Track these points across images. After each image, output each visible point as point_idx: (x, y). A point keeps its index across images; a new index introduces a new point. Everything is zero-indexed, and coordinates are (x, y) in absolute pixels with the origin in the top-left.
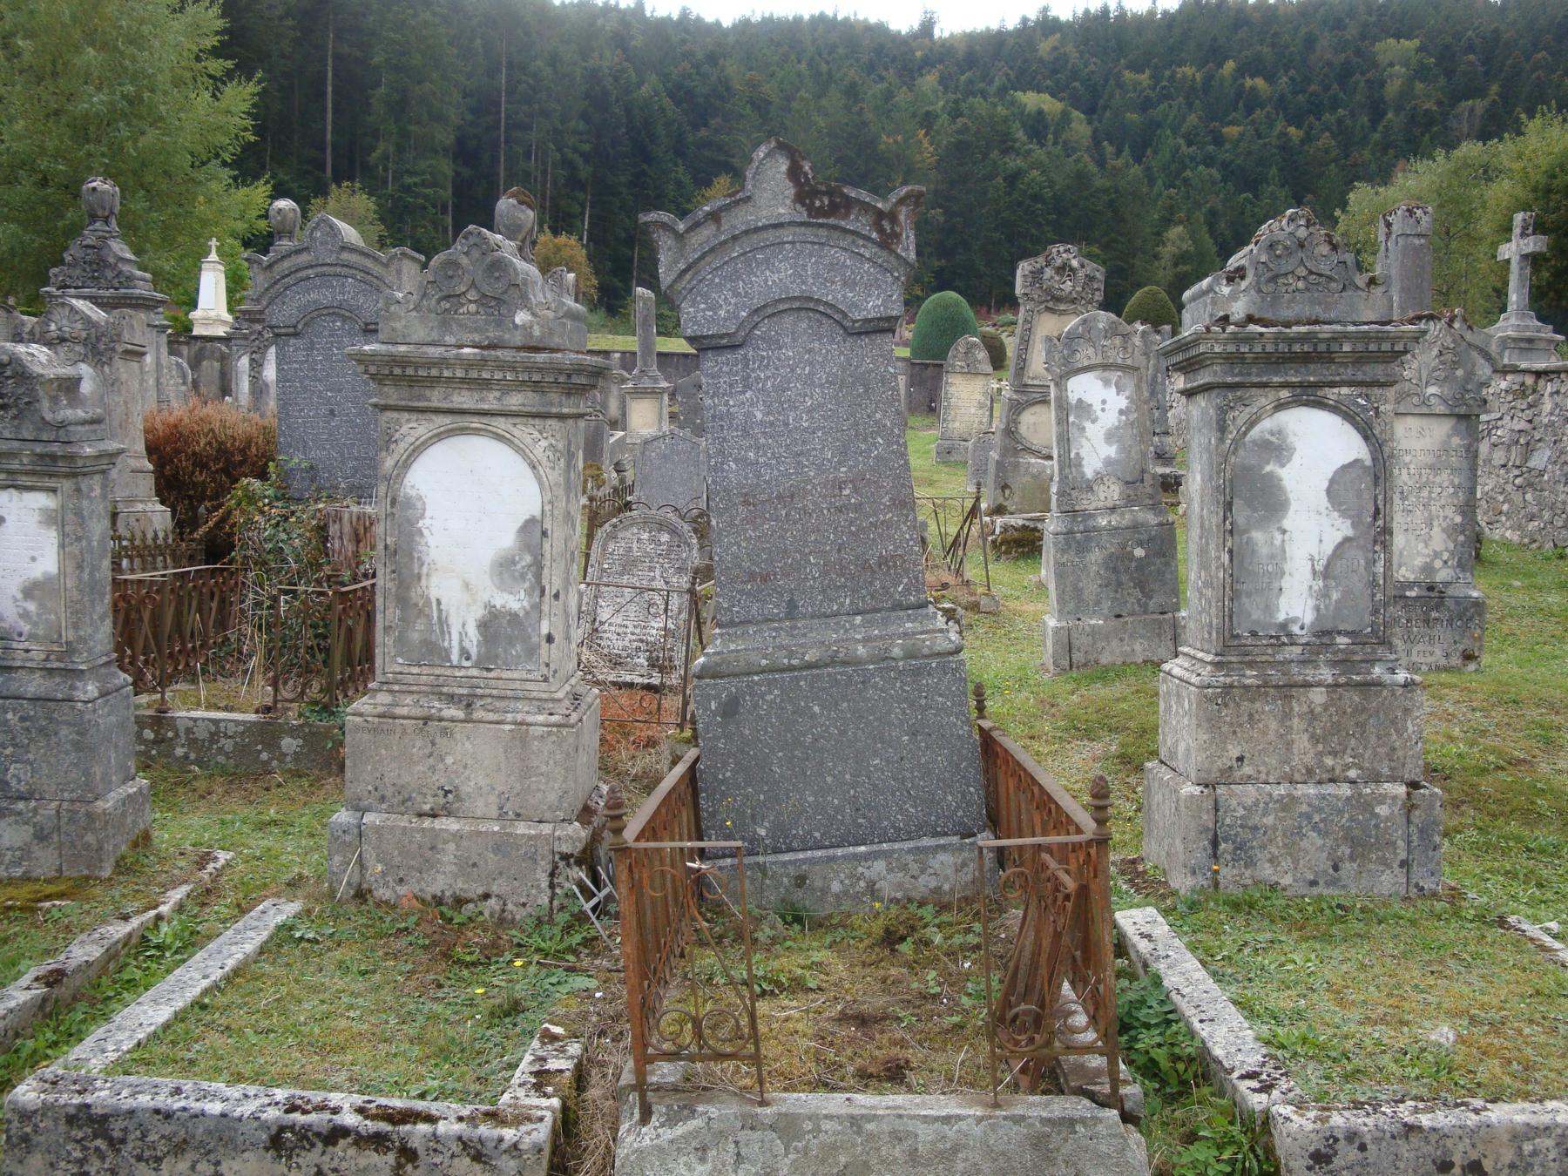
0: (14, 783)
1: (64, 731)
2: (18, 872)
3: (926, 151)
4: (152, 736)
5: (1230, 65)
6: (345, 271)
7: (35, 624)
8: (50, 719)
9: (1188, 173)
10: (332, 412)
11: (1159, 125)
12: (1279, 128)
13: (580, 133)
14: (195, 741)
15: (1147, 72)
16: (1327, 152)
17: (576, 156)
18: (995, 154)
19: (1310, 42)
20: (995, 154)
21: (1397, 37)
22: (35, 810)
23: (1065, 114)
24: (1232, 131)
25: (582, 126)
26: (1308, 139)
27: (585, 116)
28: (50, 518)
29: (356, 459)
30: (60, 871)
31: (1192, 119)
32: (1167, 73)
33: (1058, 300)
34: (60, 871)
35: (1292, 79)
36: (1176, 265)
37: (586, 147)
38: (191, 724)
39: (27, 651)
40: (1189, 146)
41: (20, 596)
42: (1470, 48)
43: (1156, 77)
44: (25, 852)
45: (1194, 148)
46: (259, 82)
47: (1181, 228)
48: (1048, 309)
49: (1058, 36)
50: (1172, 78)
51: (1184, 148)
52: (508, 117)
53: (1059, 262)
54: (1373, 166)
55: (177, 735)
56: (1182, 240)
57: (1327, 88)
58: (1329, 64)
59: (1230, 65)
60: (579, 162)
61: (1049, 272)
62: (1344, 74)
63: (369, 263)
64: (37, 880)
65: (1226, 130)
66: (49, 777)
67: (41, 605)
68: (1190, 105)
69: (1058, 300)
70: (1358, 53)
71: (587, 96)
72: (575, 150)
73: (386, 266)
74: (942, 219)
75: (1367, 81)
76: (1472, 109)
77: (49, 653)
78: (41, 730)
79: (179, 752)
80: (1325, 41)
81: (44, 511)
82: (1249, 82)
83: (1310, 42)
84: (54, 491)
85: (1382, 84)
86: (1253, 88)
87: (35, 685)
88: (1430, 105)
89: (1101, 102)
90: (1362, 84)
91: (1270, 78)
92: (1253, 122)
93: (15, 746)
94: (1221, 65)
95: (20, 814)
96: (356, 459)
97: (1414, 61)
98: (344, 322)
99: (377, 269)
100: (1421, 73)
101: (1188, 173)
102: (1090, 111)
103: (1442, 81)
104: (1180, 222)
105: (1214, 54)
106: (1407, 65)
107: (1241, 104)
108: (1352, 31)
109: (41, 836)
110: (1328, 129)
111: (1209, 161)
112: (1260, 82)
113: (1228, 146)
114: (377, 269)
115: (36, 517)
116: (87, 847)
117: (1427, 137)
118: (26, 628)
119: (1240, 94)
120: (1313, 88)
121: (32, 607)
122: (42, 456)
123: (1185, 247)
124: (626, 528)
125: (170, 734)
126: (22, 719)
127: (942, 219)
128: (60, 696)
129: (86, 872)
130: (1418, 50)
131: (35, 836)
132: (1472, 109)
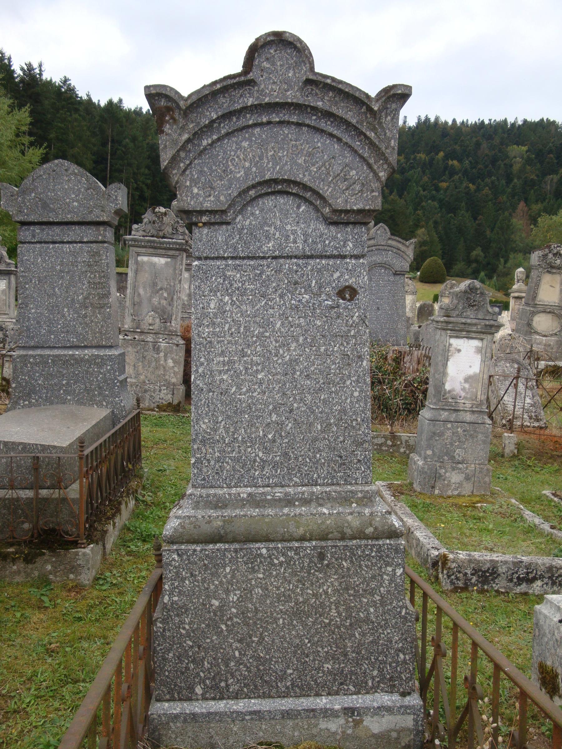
0: (457, 457)
1: (480, 436)
2: (456, 493)
4: (391, 443)
5: (441, 154)
6: (389, 248)
7: (467, 393)
8: (475, 431)
9: (424, 204)
10: (378, 308)
11: (409, 180)
12: (464, 185)
13: (146, 175)
14: (409, 446)
15: (403, 155)
16: (487, 196)
17: (144, 186)
21: (518, 145)
22: (467, 468)
24: (444, 185)
25: (147, 171)
26: (478, 190)
27: (148, 167)
28: (479, 350)
29: (388, 329)
30: (472, 492)
31: (425, 179)
32: (412, 157)
33: (552, 267)
34: (472, 492)
35: (470, 162)
36: (421, 246)
37: (149, 182)
38: (408, 438)
39: (464, 404)
40: (424, 191)
41: (463, 381)
42: (550, 152)
44: (460, 484)
45: (426, 192)
46: (45, 148)
47: (423, 229)
48: (548, 272)
50: (415, 159)
51: (422, 192)
52: (111, 166)
53: (555, 251)
54: (508, 204)
55: (401, 443)
56: (424, 235)
57: (486, 167)
58: (487, 155)
59: (441, 154)
60: (145, 188)
61: (550, 256)
62: (494, 161)
63: (400, 246)
64: (464, 496)
65: (440, 184)
66: (471, 454)
67: (471, 385)
68: (424, 172)
69: (552, 267)
70: (500, 151)
71: (149, 157)
72: (143, 183)
73: (408, 247)
75: (505, 164)
76: (552, 179)
77: (473, 404)
78: (471, 435)
79: (402, 450)
80: (485, 145)
81: (477, 347)
82: (450, 162)
83: (478, 145)
84: (482, 339)
85: (511, 166)
86: (452, 165)
87: (468, 417)
88: (532, 177)
90: (502, 166)
91: (460, 161)
92: (453, 181)
93: (459, 442)
94: (437, 154)
95: (460, 469)
96: (388, 329)
97: (525, 156)
98: (385, 270)
99: (403, 248)
100: (529, 161)
101: (424, 204)
103: (538, 165)
104: (422, 227)
105: (434, 149)
106: (522, 158)
107: (447, 172)
108: (497, 140)
109: (467, 478)
110: (487, 186)
111: (433, 198)
112: (455, 162)
113: (442, 192)
114: (403, 248)
115: (474, 350)
116: (485, 483)
117: (532, 191)
118: (463, 394)
119: (446, 168)
120: (480, 166)
121: (467, 386)
122: (486, 325)
123: (425, 238)
124: (499, 362)
125: (399, 443)
126: (464, 431)
128: (480, 422)
129: (483, 493)
130: (527, 152)
131: (465, 478)
132: (552, 179)
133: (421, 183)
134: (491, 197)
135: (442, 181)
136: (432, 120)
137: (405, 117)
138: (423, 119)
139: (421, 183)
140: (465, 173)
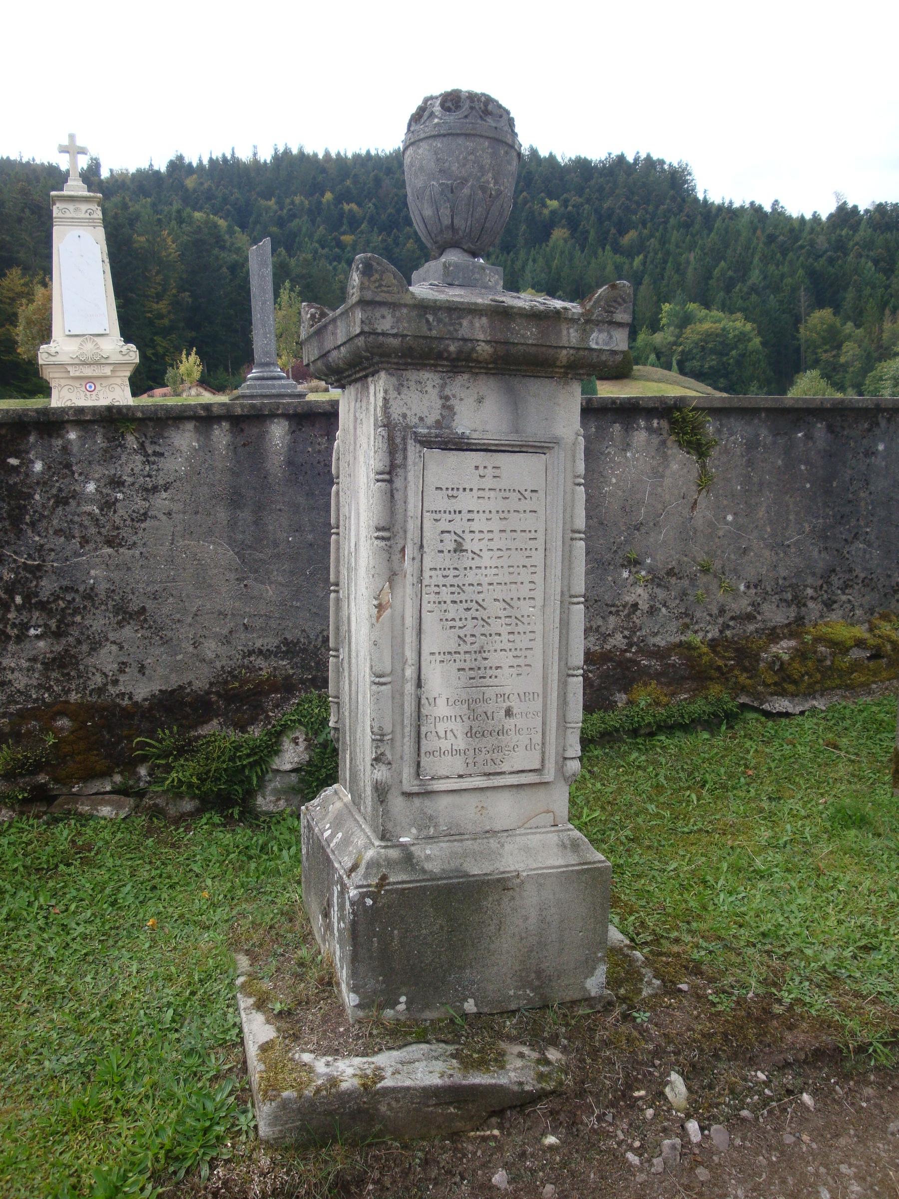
3: (171, 249)
15: (273, 200)
18: (216, 251)
19: (378, 181)
20: (216, 251)
23: (230, 227)
31: (321, 230)
32: (288, 201)
40: (323, 248)
43: (281, 204)
45: (326, 250)
49: (195, 176)
50: (293, 203)
51: (320, 250)
59: (328, 196)
65: (343, 238)
68: (313, 221)
74: (190, 300)
82: (346, 207)
83: (378, 181)
86: (350, 211)
89: (251, 220)
91: (359, 205)
92: (362, 232)
94: (323, 195)
102: (243, 227)
105: (315, 188)
107: (345, 221)
112: (353, 206)
113: (349, 248)
119: (342, 214)
120: (391, 210)
127: (190, 300)
133: (316, 238)
134: (418, 252)
135: (344, 233)
136: (295, 151)
137: (255, 147)
138: (281, 150)
139: (316, 238)
140: (372, 221)
